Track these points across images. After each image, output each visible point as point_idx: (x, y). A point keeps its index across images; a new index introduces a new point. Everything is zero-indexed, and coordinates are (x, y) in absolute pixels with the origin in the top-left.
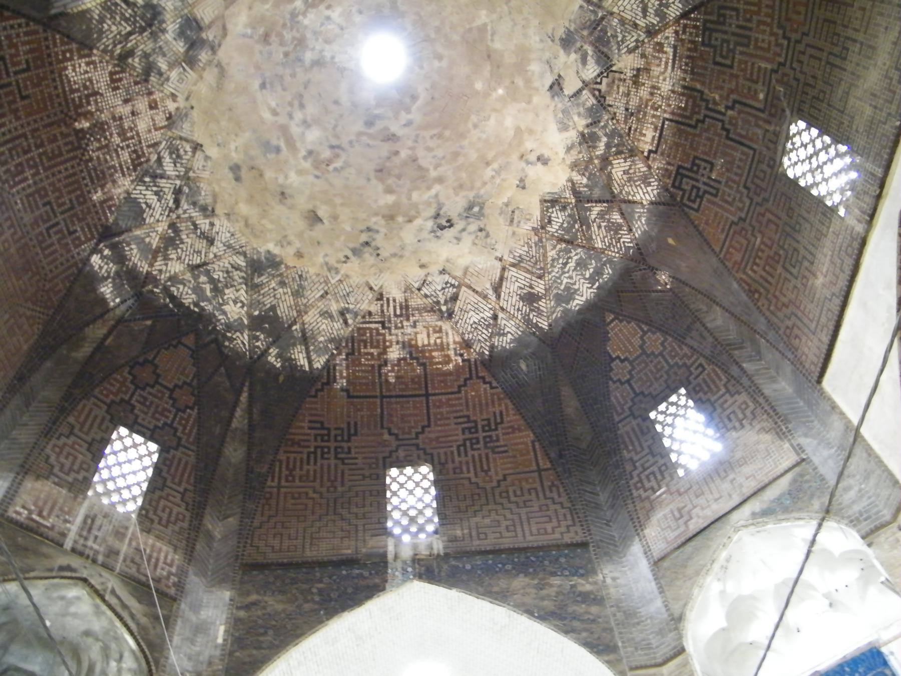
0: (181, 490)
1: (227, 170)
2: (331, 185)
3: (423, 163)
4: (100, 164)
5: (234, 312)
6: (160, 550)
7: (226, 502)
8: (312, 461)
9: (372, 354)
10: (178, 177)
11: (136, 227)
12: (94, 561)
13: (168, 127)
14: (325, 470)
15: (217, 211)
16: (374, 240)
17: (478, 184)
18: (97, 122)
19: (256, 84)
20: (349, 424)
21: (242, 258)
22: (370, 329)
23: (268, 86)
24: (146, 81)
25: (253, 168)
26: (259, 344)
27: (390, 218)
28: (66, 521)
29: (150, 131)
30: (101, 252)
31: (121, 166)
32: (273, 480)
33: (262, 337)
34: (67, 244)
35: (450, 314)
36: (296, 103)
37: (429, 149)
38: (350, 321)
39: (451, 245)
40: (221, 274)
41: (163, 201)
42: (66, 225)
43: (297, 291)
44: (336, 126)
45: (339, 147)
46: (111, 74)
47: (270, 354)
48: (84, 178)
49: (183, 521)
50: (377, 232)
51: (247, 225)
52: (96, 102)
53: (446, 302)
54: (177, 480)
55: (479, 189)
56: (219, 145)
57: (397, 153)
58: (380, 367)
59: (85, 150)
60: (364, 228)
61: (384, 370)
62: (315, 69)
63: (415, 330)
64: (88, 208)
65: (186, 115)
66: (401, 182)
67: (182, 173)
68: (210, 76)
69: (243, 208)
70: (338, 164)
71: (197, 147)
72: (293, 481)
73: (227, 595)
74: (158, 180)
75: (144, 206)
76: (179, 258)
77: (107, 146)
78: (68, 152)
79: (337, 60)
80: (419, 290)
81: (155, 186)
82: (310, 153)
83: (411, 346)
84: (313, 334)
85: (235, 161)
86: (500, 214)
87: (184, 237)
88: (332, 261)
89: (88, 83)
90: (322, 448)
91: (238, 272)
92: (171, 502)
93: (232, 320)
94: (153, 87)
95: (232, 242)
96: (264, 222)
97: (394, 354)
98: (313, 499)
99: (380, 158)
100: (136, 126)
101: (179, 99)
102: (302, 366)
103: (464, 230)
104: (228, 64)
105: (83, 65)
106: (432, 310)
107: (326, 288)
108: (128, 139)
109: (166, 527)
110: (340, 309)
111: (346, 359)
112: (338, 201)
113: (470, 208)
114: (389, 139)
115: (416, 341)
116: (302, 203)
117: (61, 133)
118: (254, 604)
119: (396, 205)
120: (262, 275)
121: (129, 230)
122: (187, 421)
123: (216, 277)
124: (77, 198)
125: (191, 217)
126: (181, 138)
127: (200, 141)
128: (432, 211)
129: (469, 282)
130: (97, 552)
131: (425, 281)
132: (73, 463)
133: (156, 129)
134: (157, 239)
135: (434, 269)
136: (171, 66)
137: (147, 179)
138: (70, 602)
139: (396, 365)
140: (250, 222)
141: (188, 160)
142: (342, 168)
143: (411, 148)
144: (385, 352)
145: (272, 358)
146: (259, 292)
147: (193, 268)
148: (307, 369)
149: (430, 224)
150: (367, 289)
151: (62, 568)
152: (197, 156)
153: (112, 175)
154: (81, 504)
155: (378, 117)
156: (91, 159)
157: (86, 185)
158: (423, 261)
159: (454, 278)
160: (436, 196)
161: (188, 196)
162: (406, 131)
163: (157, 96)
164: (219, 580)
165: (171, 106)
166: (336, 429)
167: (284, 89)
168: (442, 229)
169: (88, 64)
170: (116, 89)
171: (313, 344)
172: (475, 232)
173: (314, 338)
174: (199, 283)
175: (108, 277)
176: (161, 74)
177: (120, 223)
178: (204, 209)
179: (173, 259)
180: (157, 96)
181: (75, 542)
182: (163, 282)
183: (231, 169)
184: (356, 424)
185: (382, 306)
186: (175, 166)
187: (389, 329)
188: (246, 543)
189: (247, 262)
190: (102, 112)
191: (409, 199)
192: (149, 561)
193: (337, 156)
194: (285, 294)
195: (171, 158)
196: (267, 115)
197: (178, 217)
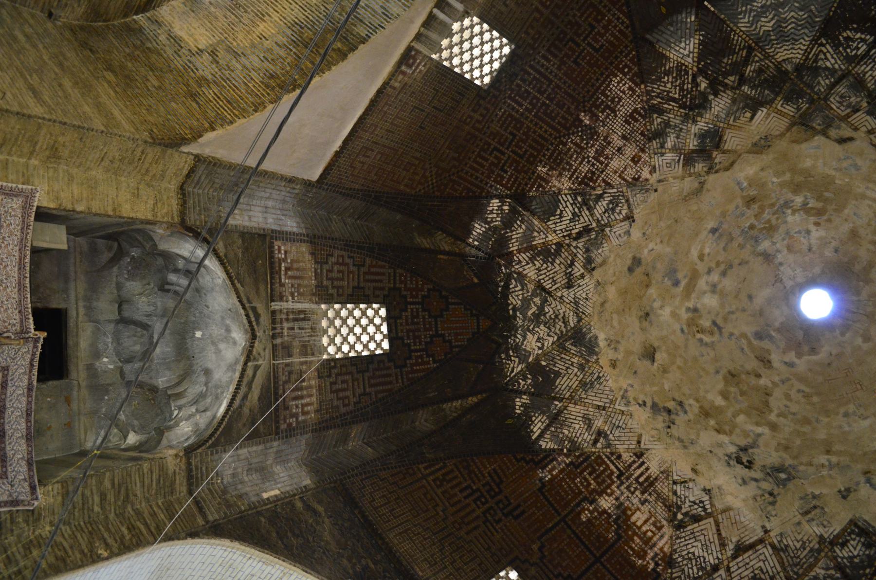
0: (367, 390)
1: (630, 256)
2: (686, 346)
3: (773, 402)
4: (566, 154)
5: (531, 344)
6: (311, 396)
7: (380, 437)
8: (465, 494)
9: (589, 484)
11: (539, 218)
12: (274, 337)
13: (629, 184)
14: (468, 510)
15: (594, 273)
16: (677, 414)
17: (804, 459)
18: (594, 128)
19: (711, 224)
20: (519, 506)
21: (576, 320)
22: (608, 466)
23: (717, 234)
24: (650, 140)
25: (647, 275)
26: (522, 383)
27: (706, 413)
28: (292, 294)
29: (616, 172)
30: (503, 202)
31: (575, 171)
32: (426, 468)
33: (529, 381)
34: (493, 172)
35: (680, 526)
36: (723, 267)
37: (788, 397)
38: (599, 445)
39: (734, 480)
40: (551, 312)
41: (572, 224)
42: (506, 162)
43: (586, 384)
44: (732, 313)
45: (719, 328)
46: (635, 110)
47: (521, 398)
48: (548, 150)
49: (344, 406)
50: (686, 412)
51: (602, 304)
52: (607, 117)
53: (686, 514)
54: (372, 381)
55: (801, 464)
56: (644, 234)
57: (759, 376)
58: (585, 499)
59: (569, 135)
60: (679, 400)
61: (586, 505)
62: (760, 258)
63: (640, 506)
64: (529, 169)
66: (740, 398)
68: (689, 184)
69: (612, 292)
70: (707, 339)
71: (630, 218)
72: (439, 487)
73: (307, 482)
74: (585, 208)
75: (558, 212)
76: (539, 270)
77: (582, 149)
78: (559, 123)
79: (782, 268)
80: (675, 483)
81: (579, 209)
82: (695, 310)
83: (624, 512)
84: (564, 421)
86: (801, 498)
87: (558, 261)
88: (631, 395)
90: (483, 496)
91: (563, 325)
92: (353, 385)
93: (523, 347)
95: (581, 302)
96: (615, 316)
97: (606, 503)
98: (438, 514)
99: (742, 366)
100: (612, 159)
101: (654, 175)
102: (532, 431)
103: (756, 480)
104: (708, 190)
106: (669, 507)
107: (608, 405)
108: (598, 161)
109: (332, 392)
110: (602, 428)
111: (568, 465)
112: (679, 362)
113: (780, 469)
114: (762, 361)
115: (633, 514)
116: (654, 335)
117: (569, 108)
118: (315, 512)
119: (719, 410)
120: (575, 346)
121: (533, 214)
122: (423, 363)
123: (547, 310)
124: (532, 155)
125: (575, 255)
126: (627, 201)
127: (635, 216)
128: (743, 442)
129: (721, 520)
130: (281, 335)
131: (685, 482)
132: (337, 279)
133: (620, 176)
134: (541, 241)
135: (702, 482)
136: (674, 149)
137: (579, 199)
138: (227, 339)
139: (598, 512)
140: (607, 305)
141: (616, 219)
142: (706, 344)
143: (773, 383)
144: (600, 494)
145: (520, 402)
146: (561, 353)
147: (540, 286)
148: (533, 438)
149: (732, 449)
150: (636, 438)
151: (254, 309)
152: (623, 224)
153: (564, 169)
154: (311, 301)
155: (771, 338)
156: (565, 144)
157: (544, 155)
158: (698, 467)
159: (712, 505)
160: (759, 435)
161: (588, 240)
162: (783, 368)
163: (645, 157)
164: (313, 466)
165: (645, 174)
166: (506, 497)
167: (724, 249)
168: (738, 462)
169: (630, 88)
170: (627, 122)
171: (556, 428)
172: (764, 490)
173: (562, 425)
174: (532, 299)
175: (488, 223)
176: (662, 147)
177: (534, 203)
178: (589, 261)
179: (535, 265)
180: (645, 157)
181: (281, 311)
182: (513, 269)
183: (634, 258)
184: (523, 512)
185: (634, 462)
186: (604, 213)
187: (622, 483)
188: (361, 474)
189: (575, 326)
190: (603, 126)
191: (734, 416)
192: (297, 389)
193: (712, 333)
194: (576, 375)
195: (608, 205)
196: (695, 253)
197: (569, 245)
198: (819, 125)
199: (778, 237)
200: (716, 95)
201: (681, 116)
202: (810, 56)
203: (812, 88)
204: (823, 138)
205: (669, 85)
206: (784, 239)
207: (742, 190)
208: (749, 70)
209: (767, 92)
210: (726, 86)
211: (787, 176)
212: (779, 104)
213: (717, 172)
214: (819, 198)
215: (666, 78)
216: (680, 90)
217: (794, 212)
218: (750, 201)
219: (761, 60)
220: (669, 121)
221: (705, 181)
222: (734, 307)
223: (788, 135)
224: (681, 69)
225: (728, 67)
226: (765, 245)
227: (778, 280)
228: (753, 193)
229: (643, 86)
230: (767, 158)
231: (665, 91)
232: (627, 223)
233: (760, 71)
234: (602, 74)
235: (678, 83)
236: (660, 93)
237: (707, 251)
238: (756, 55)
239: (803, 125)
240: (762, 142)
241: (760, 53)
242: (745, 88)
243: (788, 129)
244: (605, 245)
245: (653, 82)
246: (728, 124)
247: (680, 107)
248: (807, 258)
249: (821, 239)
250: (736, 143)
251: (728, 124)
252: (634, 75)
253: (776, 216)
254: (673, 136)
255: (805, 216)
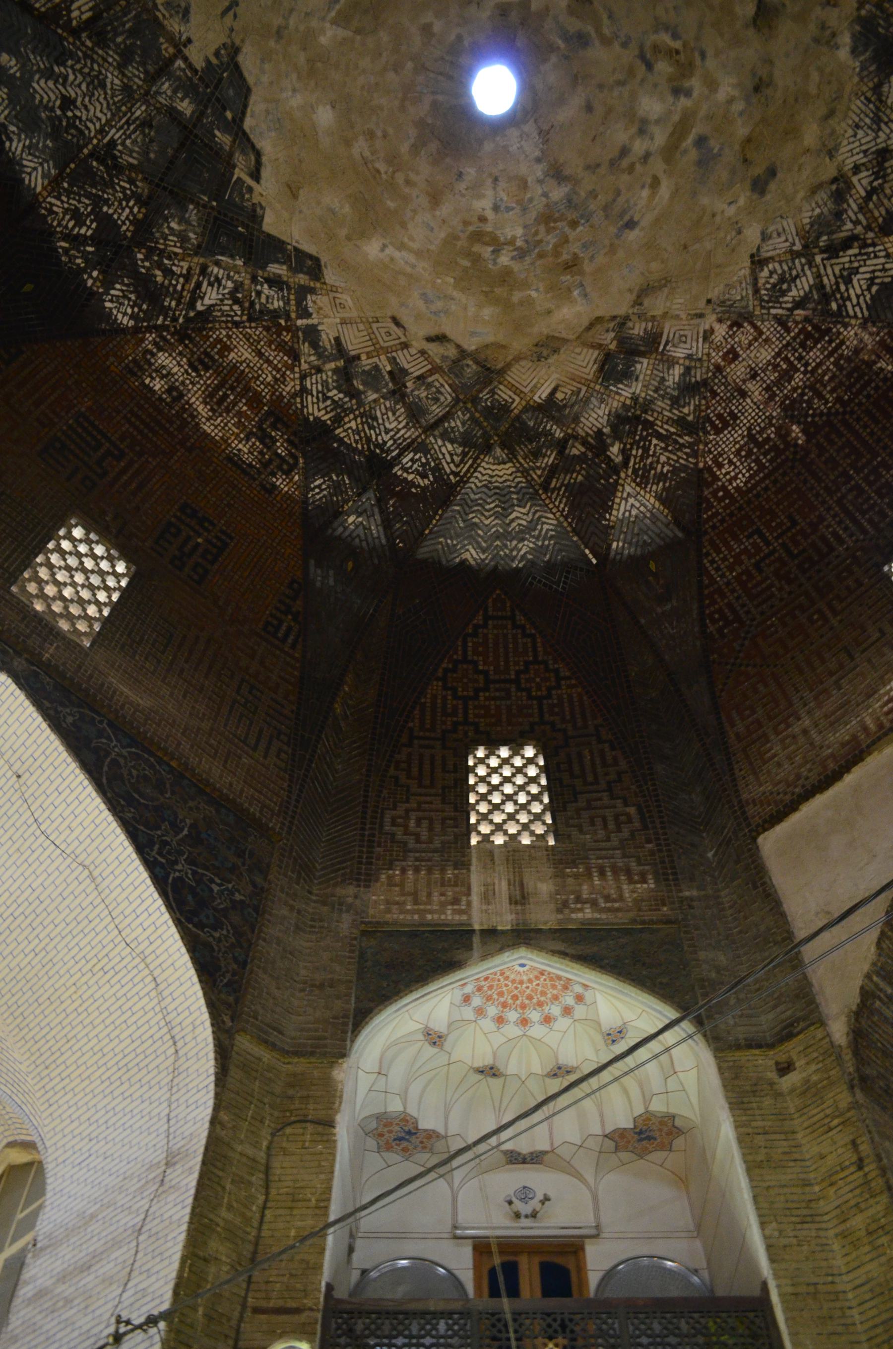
1: (768, 197)
10: (811, 263)
13: (748, 317)
19: (633, 235)
23: (627, 218)
24: (705, 383)
25: (745, 161)
29: (767, 340)
36: (625, 163)
46: (718, 431)
52: (763, 430)
56: (739, 232)
62: (567, 172)
65: (722, 303)
67: (803, 260)
68: (657, 305)
69: (811, 135)
71: (758, 262)
77: (812, 388)
79: (537, 153)
85: (748, 194)
89: (743, 453)
94: (708, 370)
100: (769, 363)
101: (707, 327)
104: (630, 290)
105: (724, 471)
108: (790, 363)
126: (756, 291)
127: (747, 263)
133: (761, 333)
136: (671, 362)
141: (780, 262)
163: (717, 358)
165: (721, 330)
167: (618, 193)
169: (720, 466)
170: (734, 417)
176: (688, 369)
180: (717, 358)
186: (797, 276)
190: (771, 418)
195: (789, 290)
196: (665, 191)
198: (468, 365)
199: (539, 205)
200: (599, 432)
201: (653, 411)
202: (470, 462)
203: (472, 419)
204: (466, 347)
205: (663, 459)
206: (531, 200)
207: (582, 285)
208: (550, 459)
209: (531, 424)
210: (584, 443)
211: (517, 297)
212: (517, 404)
213: (614, 318)
214: (476, 259)
215: (665, 470)
216: (649, 449)
217: (511, 242)
218: (572, 266)
219: (533, 469)
220: (672, 406)
221: (633, 306)
222: (616, 93)
223: (510, 357)
224: (643, 479)
225: (578, 468)
226: (558, 193)
227: (544, 134)
228: (567, 278)
229: (701, 465)
230: (541, 328)
231: (670, 452)
232: (765, 255)
233: (536, 454)
234: (758, 496)
235: (650, 460)
236: (678, 450)
237: (645, 193)
238: (539, 477)
239: (488, 369)
240: (545, 353)
241: (533, 479)
242: (559, 434)
243: (508, 366)
244: (807, 221)
245: (684, 468)
246: (588, 386)
247: (652, 424)
248: (501, 166)
249: (481, 196)
250: (581, 357)
251: (588, 386)
252: (709, 485)
253: (538, 238)
254: (670, 383)
255: (498, 233)
